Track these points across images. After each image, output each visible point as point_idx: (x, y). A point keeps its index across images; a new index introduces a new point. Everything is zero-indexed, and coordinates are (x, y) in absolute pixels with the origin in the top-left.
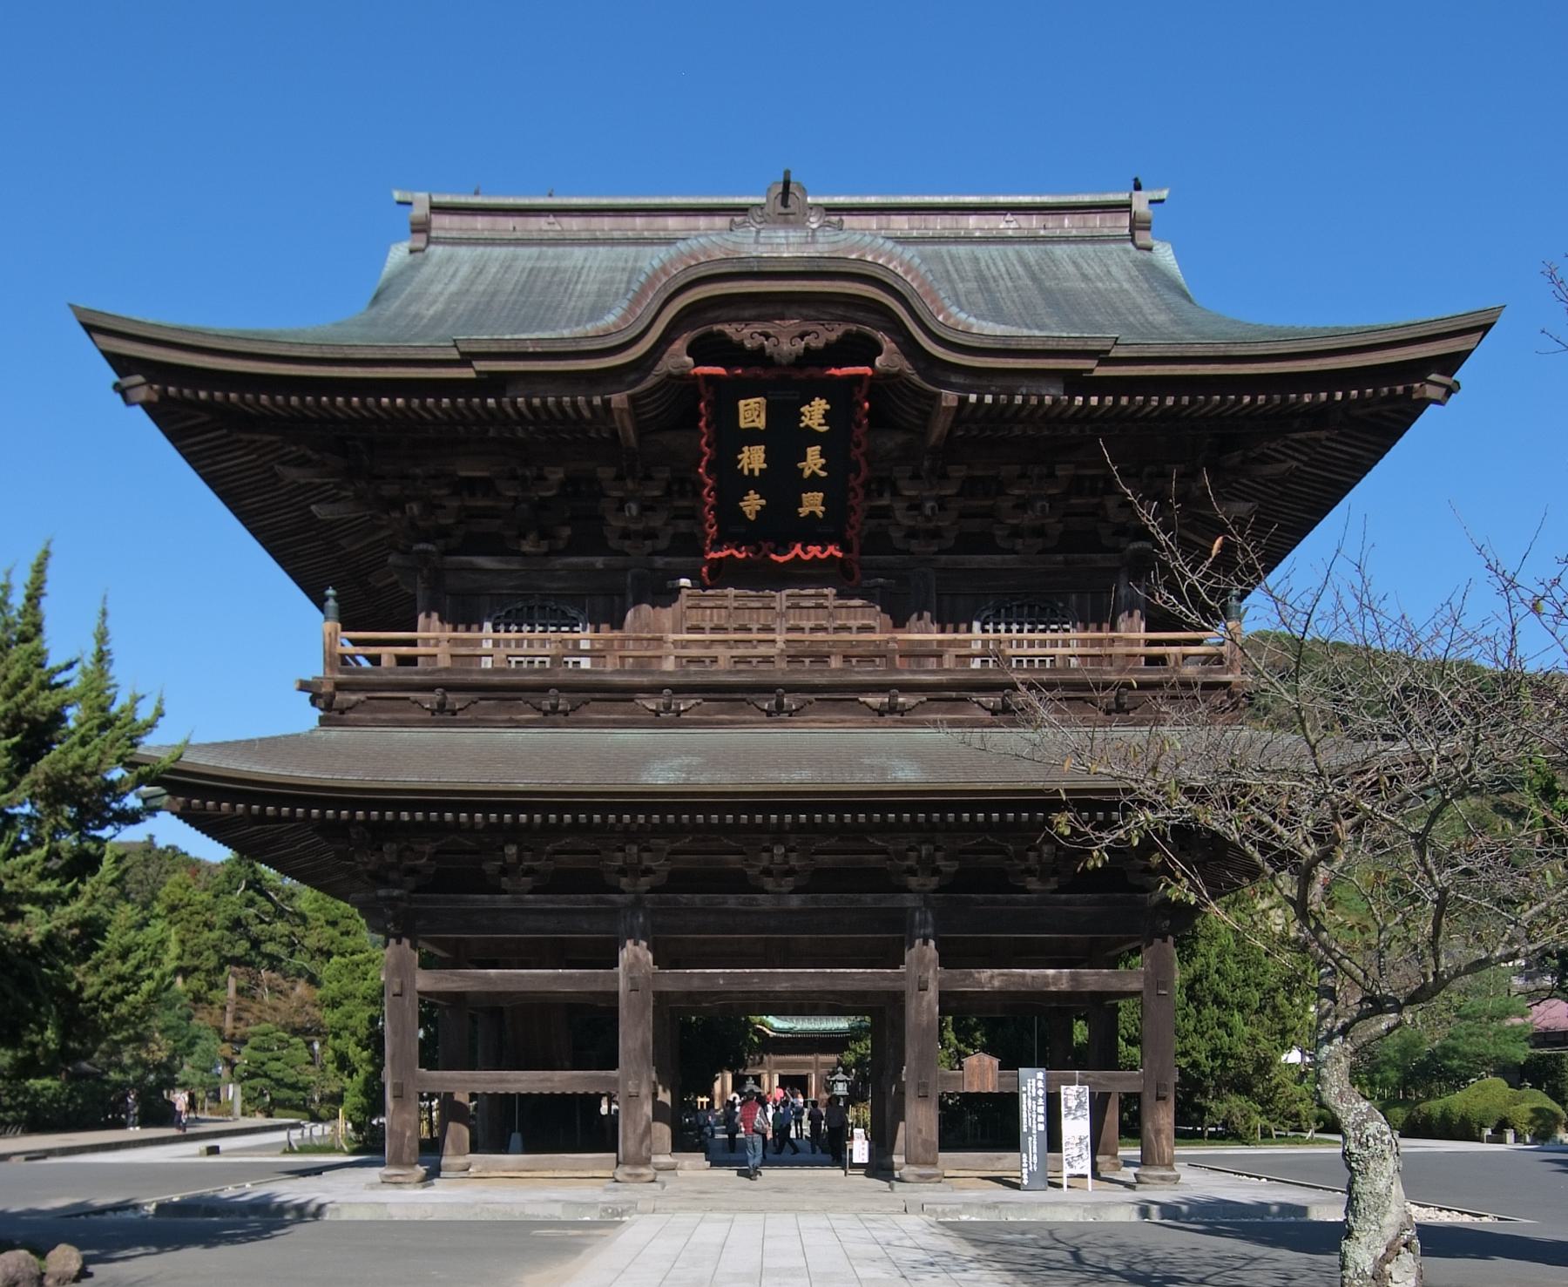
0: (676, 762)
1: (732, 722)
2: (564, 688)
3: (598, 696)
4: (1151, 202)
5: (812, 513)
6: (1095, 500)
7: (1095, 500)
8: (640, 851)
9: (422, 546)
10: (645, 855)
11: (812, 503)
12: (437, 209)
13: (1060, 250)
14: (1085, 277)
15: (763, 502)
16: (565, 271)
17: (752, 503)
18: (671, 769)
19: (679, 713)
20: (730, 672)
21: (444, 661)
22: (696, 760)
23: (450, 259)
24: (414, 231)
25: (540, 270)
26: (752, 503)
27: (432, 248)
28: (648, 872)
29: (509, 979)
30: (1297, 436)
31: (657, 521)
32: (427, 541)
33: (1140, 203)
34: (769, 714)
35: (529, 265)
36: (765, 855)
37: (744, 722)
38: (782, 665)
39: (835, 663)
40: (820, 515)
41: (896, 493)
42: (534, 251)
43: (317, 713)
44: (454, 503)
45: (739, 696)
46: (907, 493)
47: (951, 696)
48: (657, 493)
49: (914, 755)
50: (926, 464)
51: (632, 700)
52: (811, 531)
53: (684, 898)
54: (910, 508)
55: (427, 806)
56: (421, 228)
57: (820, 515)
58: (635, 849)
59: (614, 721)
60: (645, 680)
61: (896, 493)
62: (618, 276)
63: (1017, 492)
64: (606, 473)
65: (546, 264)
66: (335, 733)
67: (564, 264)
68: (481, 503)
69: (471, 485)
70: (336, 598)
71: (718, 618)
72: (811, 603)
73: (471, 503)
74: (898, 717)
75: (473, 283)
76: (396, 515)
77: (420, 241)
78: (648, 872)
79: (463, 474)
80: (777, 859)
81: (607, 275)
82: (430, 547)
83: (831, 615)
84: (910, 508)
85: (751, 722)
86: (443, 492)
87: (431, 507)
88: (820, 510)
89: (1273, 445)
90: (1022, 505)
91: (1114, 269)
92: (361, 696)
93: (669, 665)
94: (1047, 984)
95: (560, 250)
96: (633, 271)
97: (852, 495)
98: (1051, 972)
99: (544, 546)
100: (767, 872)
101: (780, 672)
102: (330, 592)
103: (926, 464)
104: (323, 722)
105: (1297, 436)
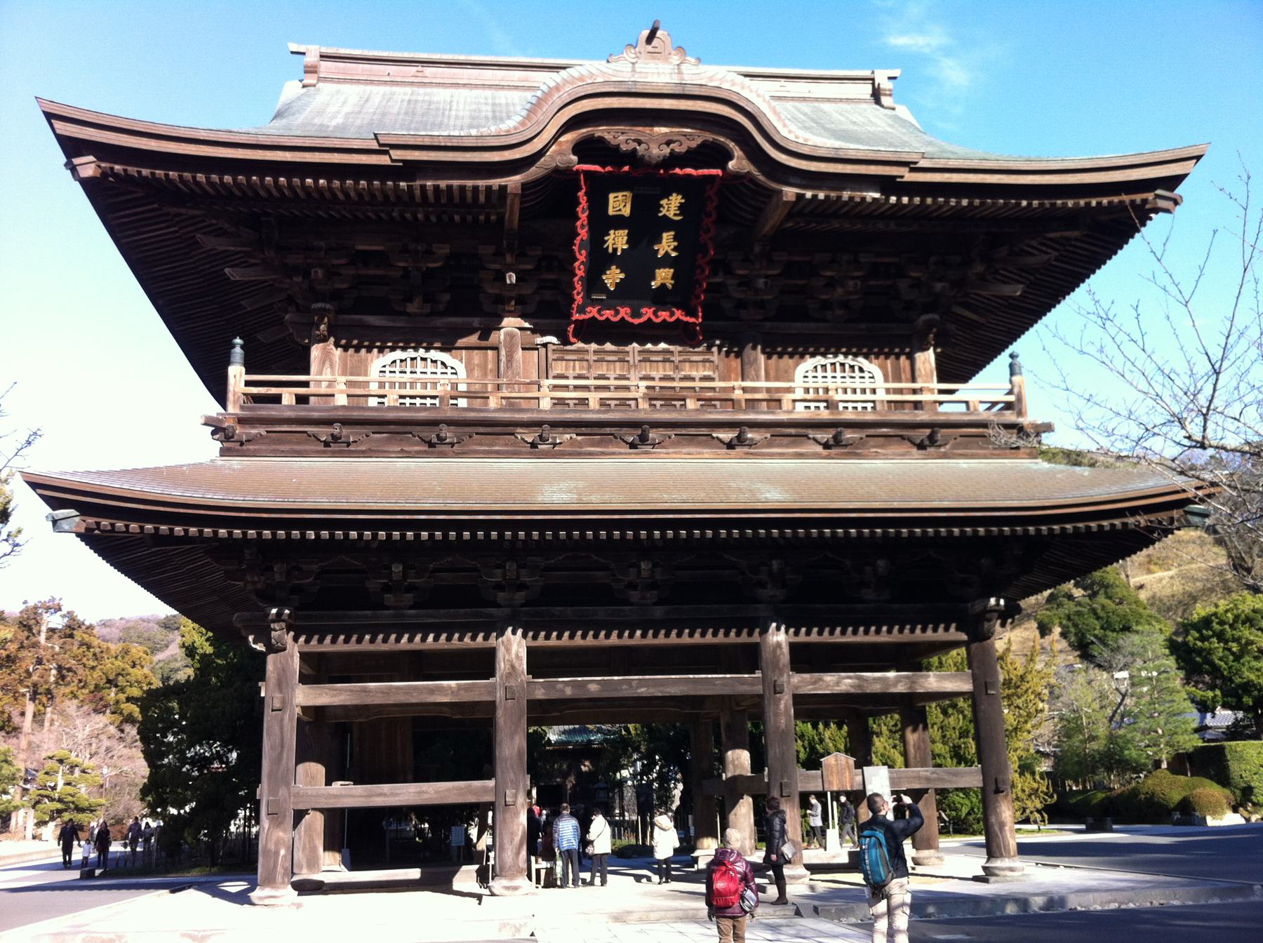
0: (564, 485)
1: (603, 454)
2: (451, 423)
3: (481, 430)
4: (890, 78)
5: (663, 285)
6: (889, 283)
7: (889, 283)
8: (520, 567)
9: (319, 305)
10: (523, 572)
11: (663, 276)
12: (323, 57)
13: (826, 107)
14: (854, 123)
15: (622, 276)
16: (438, 102)
17: (613, 276)
18: (561, 491)
19: (555, 445)
20: (598, 412)
21: (341, 400)
22: (581, 484)
23: (338, 92)
24: (306, 72)
25: (416, 101)
26: (613, 276)
27: (321, 85)
28: (522, 587)
29: (408, 691)
30: (1052, 235)
31: (527, 290)
32: (323, 301)
33: (881, 79)
34: (633, 446)
35: (407, 98)
36: (633, 571)
37: (614, 454)
38: (644, 405)
39: (691, 404)
40: (670, 286)
41: (729, 272)
42: (408, 90)
43: (219, 445)
44: (351, 271)
45: (608, 430)
46: (740, 272)
47: (793, 432)
48: (529, 267)
49: (771, 479)
50: (757, 249)
51: (513, 434)
52: (661, 298)
53: (557, 610)
54: (739, 285)
55: (332, 525)
56: (311, 70)
57: (670, 286)
58: (515, 566)
59: (497, 452)
60: (525, 416)
61: (729, 272)
62: (484, 108)
63: (829, 274)
64: (486, 250)
65: (420, 98)
66: (236, 462)
67: (435, 99)
68: (373, 272)
69: (366, 258)
70: (242, 347)
71: (579, 369)
72: (660, 358)
73: (363, 272)
74: (746, 449)
75: (362, 107)
76: (298, 279)
77: (310, 80)
78: (522, 587)
79: (360, 247)
80: (644, 574)
81: (474, 107)
82: (328, 306)
83: (677, 368)
84: (739, 285)
85: (620, 454)
86: (342, 261)
87: (331, 274)
88: (669, 283)
89: (1034, 243)
90: (831, 284)
91: (873, 119)
92: (262, 430)
93: (546, 404)
94: (888, 686)
95: (429, 90)
96: (494, 104)
97: (698, 271)
98: (892, 674)
99: (427, 309)
100: (632, 586)
101: (644, 411)
102: (238, 341)
103: (757, 249)
104: (224, 452)
105: (1052, 235)
